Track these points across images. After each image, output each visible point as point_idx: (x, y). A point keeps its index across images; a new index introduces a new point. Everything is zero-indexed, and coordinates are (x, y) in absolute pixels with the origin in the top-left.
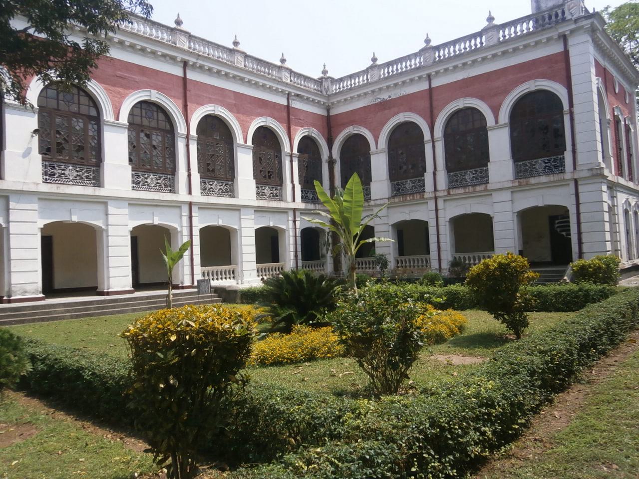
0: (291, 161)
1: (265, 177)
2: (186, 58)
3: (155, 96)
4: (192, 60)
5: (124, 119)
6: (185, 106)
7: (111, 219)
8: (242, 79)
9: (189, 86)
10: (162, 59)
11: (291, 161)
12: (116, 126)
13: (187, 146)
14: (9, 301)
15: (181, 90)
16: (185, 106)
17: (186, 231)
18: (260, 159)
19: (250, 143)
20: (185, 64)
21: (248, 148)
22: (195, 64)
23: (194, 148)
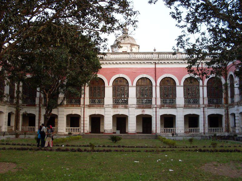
0: (203, 89)
1: (190, 96)
2: (155, 62)
3: (145, 76)
4: (157, 62)
5: (135, 84)
6: (156, 76)
7: (130, 113)
8: (179, 63)
9: (156, 70)
10: (147, 64)
11: (203, 89)
12: (132, 86)
13: (156, 89)
14: (104, 134)
15: (154, 72)
16: (156, 76)
17: (155, 116)
18: (188, 89)
19: (182, 84)
20: (155, 63)
21: (181, 86)
22: (158, 63)
23: (158, 89)
